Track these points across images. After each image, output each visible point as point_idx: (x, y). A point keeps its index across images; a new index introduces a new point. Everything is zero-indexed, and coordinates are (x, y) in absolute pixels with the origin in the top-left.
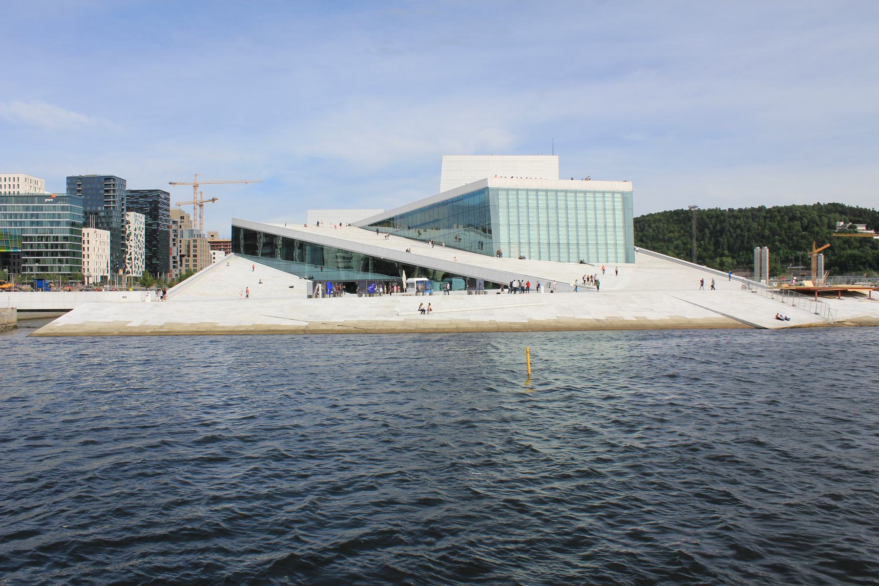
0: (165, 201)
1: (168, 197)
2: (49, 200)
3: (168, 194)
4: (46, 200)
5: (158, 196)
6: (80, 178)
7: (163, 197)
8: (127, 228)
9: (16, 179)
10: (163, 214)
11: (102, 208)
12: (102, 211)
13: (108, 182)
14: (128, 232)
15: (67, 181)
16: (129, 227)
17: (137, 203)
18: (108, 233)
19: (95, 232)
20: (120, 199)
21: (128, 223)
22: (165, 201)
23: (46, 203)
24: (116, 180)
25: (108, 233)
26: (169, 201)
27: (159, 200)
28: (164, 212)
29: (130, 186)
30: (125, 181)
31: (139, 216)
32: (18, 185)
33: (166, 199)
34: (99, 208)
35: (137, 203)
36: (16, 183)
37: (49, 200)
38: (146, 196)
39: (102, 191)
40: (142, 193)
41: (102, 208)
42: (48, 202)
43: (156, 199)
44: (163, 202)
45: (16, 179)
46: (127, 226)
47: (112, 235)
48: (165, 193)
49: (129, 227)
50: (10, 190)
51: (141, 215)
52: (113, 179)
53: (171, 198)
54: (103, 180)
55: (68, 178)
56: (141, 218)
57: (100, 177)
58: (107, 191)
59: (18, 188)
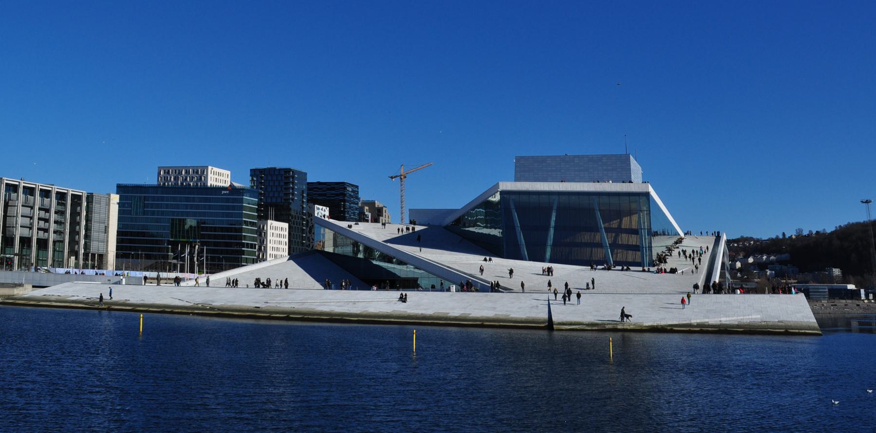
3: (357, 187)
4: (223, 192)
5: (345, 188)
16: (311, 220)
17: (325, 195)
18: (285, 225)
19: (272, 224)
22: (352, 194)
23: (222, 195)
25: (285, 225)
26: (358, 193)
27: (345, 193)
29: (310, 179)
31: (322, 209)
35: (325, 195)
38: (333, 189)
43: (343, 192)
44: (350, 195)
47: (290, 227)
48: (353, 185)
49: (311, 220)
51: (324, 208)
54: (283, 173)
56: (325, 211)
57: (280, 170)
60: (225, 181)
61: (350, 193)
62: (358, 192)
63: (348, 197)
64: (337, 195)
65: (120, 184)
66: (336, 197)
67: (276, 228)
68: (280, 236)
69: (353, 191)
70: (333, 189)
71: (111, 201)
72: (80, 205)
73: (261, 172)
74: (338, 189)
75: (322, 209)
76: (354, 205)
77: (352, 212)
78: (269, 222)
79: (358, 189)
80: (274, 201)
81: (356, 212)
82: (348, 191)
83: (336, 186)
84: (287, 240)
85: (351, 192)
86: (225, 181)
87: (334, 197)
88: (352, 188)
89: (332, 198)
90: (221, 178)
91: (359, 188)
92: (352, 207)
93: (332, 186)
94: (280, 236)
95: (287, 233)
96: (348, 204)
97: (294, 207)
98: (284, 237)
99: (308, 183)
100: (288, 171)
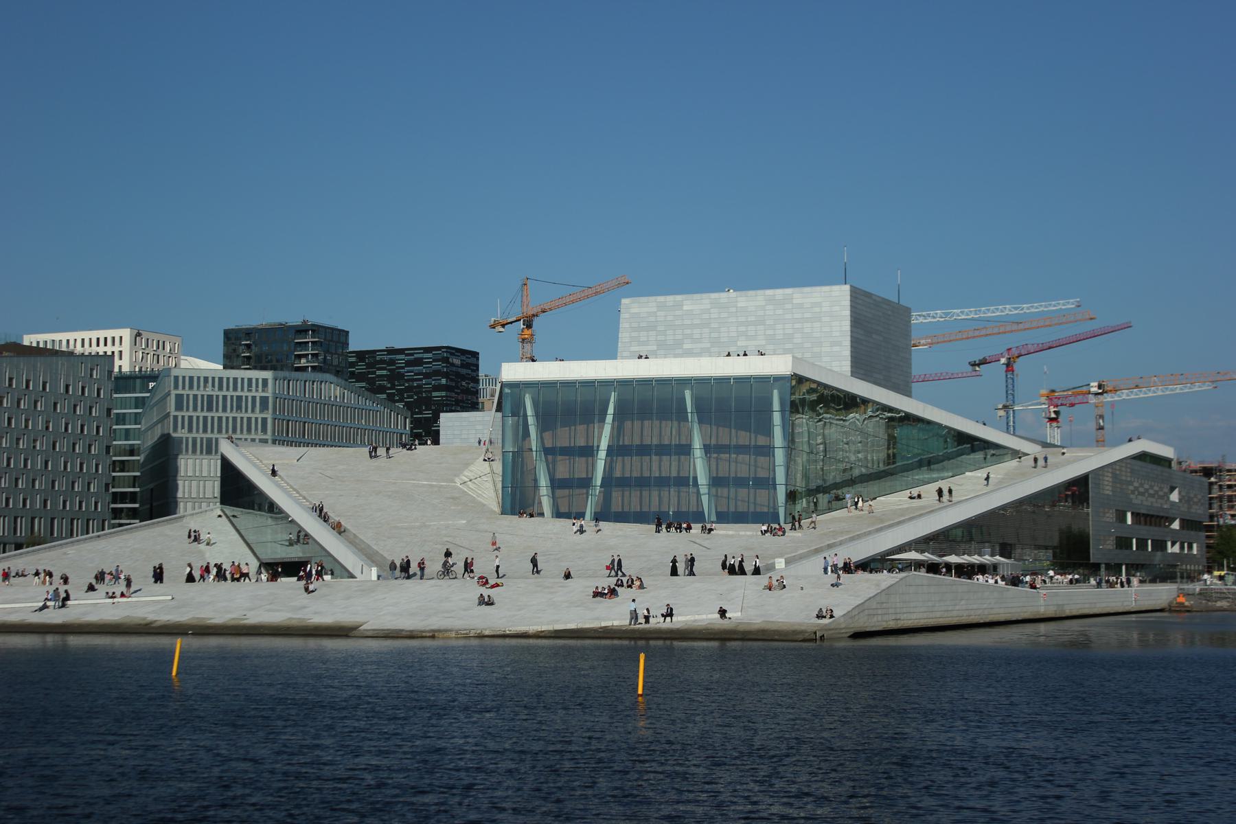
1: (472, 360)
3: (475, 355)
7: (457, 361)
9: (117, 341)
22: (464, 371)
26: (478, 370)
32: (121, 352)
38: (419, 362)
40: (412, 355)
45: (117, 341)
62: (477, 366)
64: (427, 376)
70: (419, 362)
79: (478, 359)
82: (453, 365)
83: (426, 355)
85: (463, 366)
88: (464, 358)
92: (462, 401)
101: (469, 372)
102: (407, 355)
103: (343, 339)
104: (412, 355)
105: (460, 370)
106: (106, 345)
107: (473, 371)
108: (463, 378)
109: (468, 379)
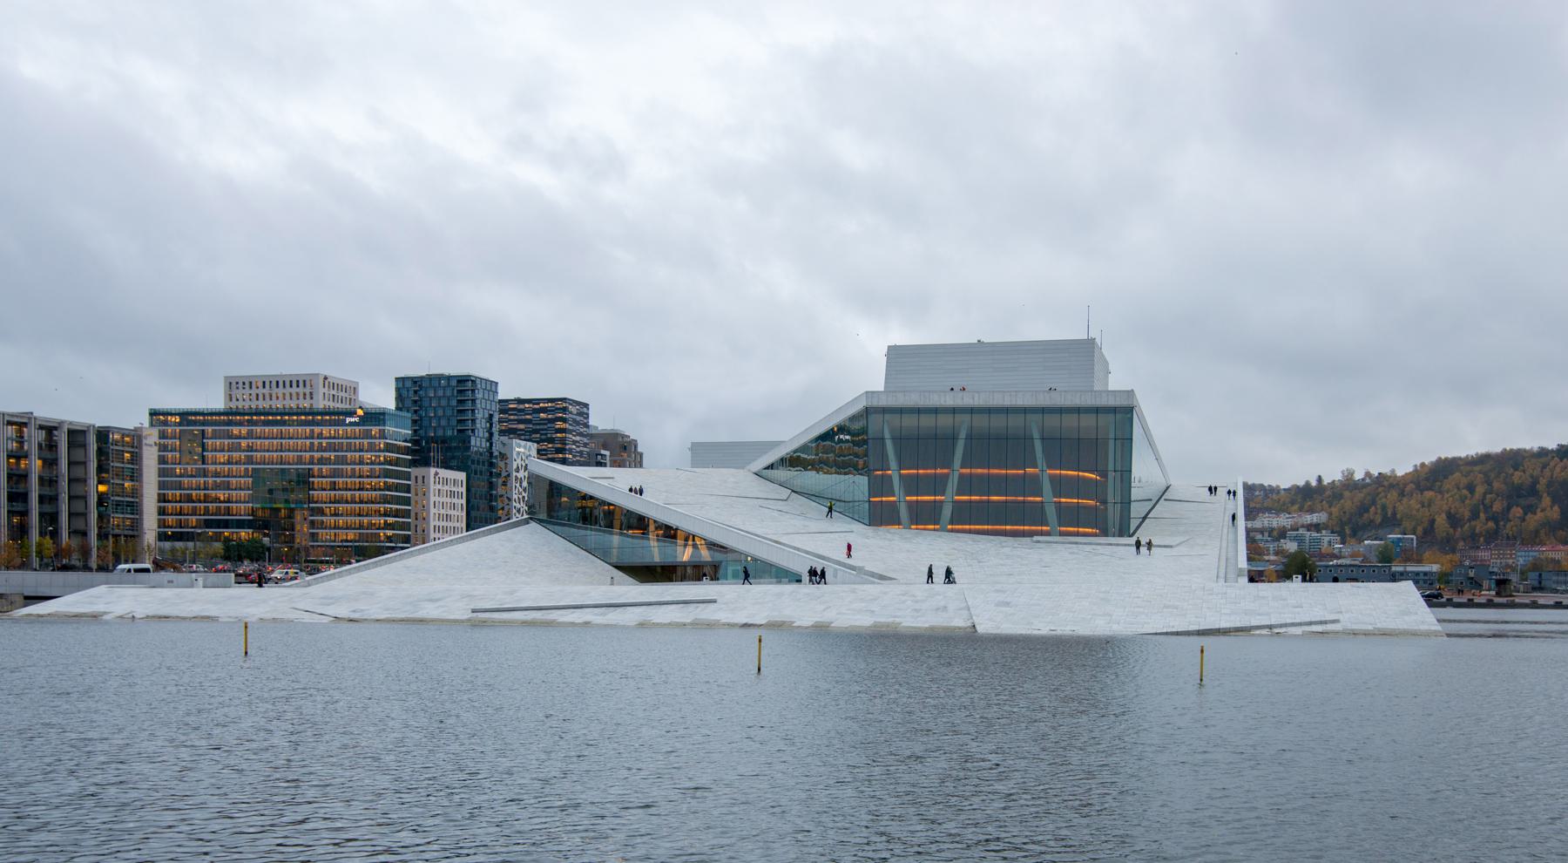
0: (578, 418)
1: (585, 410)
2: (353, 420)
3: (586, 406)
5: (565, 410)
6: (416, 381)
8: (503, 466)
10: (574, 442)
11: (453, 432)
12: (451, 438)
13: (464, 388)
14: (504, 474)
15: (397, 384)
18: (462, 476)
19: (436, 474)
20: (487, 416)
21: (503, 456)
22: (578, 418)
24: (478, 381)
26: (588, 417)
27: (567, 417)
28: (578, 438)
29: (503, 394)
30: (497, 383)
32: (311, 393)
33: (580, 414)
34: (449, 433)
36: (308, 391)
37: (353, 420)
39: (454, 403)
41: (453, 432)
42: (351, 424)
44: (574, 421)
46: (502, 464)
50: (271, 403)
52: (472, 381)
53: (590, 412)
54: (454, 383)
55: (396, 379)
57: (449, 378)
58: (460, 402)
59: (312, 398)
60: (350, 399)
61: (574, 417)
62: (588, 414)
63: (570, 424)
65: (155, 410)
66: (549, 425)
67: (446, 481)
68: (452, 494)
69: (580, 414)
71: (144, 441)
72: (84, 446)
73: (415, 382)
74: (553, 411)
75: (525, 448)
76: (582, 438)
77: (578, 449)
78: (433, 470)
79: (588, 409)
80: (440, 433)
81: (585, 449)
82: (571, 413)
84: (464, 501)
86: (350, 399)
87: (545, 424)
89: (542, 427)
90: (342, 394)
91: (590, 407)
93: (541, 405)
94: (452, 494)
95: (464, 490)
96: (571, 436)
97: (478, 443)
98: (459, 495)
99: (500, 401)
100: (463, 380)
101: (582, 418)
102: (534, 404)
103: (493, 389)
104: (538, 404)
105: (574, 417)
106: (298, 386)
107: (585, 418)
108: (578, 423)
109: (582, 424)
